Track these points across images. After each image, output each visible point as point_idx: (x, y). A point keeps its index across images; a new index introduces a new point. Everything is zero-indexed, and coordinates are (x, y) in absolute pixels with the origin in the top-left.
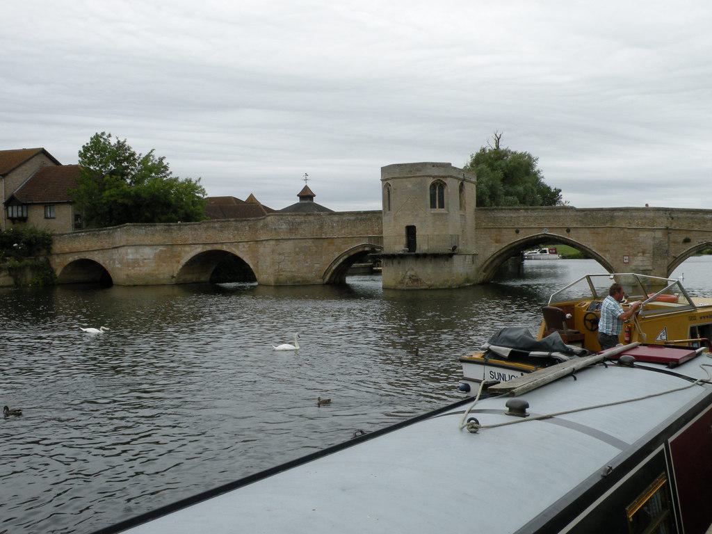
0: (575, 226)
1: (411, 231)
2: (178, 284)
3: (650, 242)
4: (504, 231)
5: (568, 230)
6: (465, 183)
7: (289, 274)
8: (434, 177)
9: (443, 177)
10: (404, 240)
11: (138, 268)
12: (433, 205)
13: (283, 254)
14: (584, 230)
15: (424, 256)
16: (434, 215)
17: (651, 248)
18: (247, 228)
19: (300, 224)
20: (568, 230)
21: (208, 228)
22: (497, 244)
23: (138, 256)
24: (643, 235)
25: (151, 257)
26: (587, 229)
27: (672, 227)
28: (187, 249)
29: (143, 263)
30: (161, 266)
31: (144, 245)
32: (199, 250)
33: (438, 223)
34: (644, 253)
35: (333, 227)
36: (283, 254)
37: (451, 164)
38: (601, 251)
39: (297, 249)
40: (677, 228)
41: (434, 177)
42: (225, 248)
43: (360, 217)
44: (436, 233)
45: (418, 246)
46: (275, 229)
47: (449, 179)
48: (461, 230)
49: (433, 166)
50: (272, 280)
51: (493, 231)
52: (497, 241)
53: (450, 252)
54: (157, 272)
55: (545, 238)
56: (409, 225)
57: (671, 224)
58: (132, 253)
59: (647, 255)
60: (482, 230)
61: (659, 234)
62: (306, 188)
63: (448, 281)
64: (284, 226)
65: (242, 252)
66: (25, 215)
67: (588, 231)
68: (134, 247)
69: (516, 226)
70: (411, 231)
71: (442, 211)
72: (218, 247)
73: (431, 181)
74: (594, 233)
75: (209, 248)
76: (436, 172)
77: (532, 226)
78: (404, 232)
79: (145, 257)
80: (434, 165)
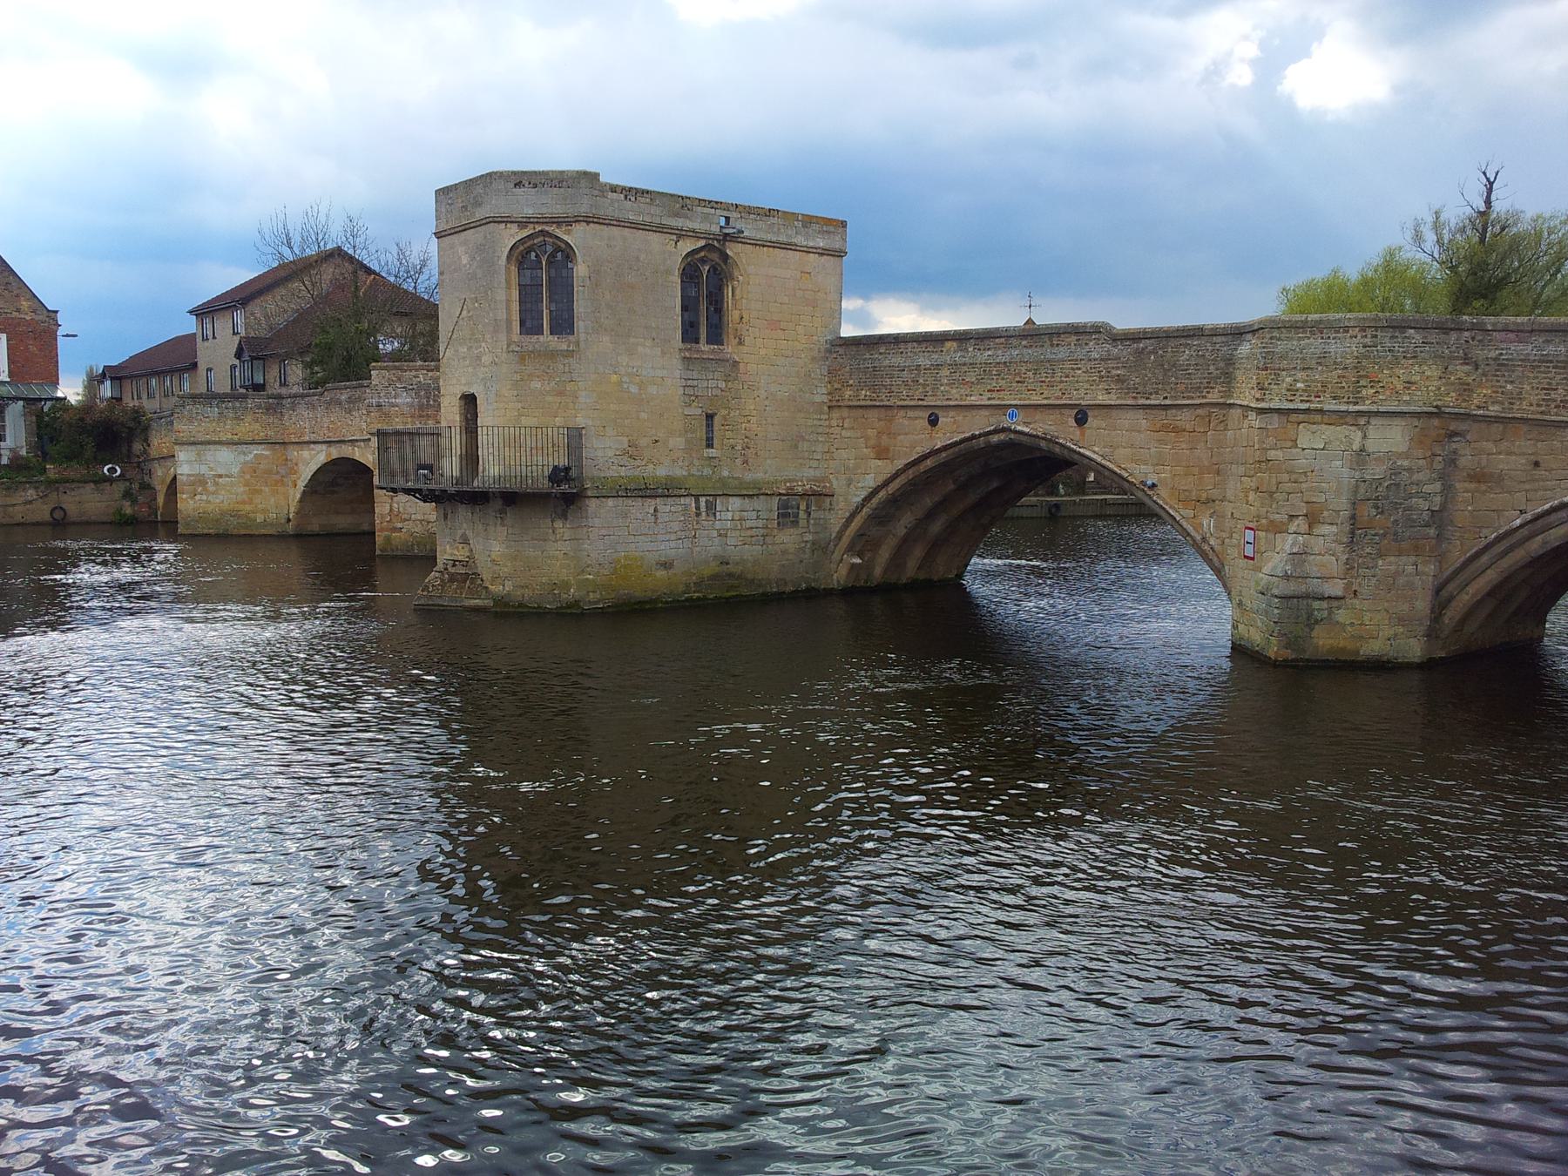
0: (1102, 398)
2: (300, 537)
3: (1340, 470)
4: (901, 419)
5: (1081, 420)
6: (732, 250)
7: (418, 529)
8: (522, 224)
11: (204, 497)
12: (530, 325)
14: (1131, 414)
17: (1342, 503)
20: (1081, 420)
22: (879, 463)
23: (204, 469)
24: (1311, 437)
25: (235, 470)
26: (1140, 413)
27: (1473, 405)
28: (306, 454)
29: (216, 484)
30: (259, 492)
31: (215, 443)
34: (1313, 519)
37: (597, 175)
40: (1494, 409)
44: (525, 421)
46: (379, 405)
47: (579, 229)
49: (518, 184)
51: (873, 415)
52: (882, 453)
54: (248, 508)
57: (1466, 389)
58: (189, 462)
59: (1326, 529)
60: (845, 412)
61: (1390, 439)
63: (566, 586)
64: (404, 399)
67: (1141, 420)
68: (193, 448)
69: (930, 401)
73: (510, 236)
74: (1165, 428)
75: (335, 452)
76: (528, 204)
77: (973, 400)
79: (220, 472)
80: (520, 180)
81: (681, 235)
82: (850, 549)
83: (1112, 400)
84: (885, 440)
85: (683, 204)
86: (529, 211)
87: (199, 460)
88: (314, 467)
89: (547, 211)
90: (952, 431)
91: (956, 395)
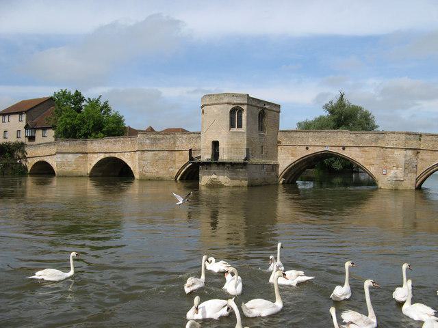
1: (216, 144)
5: (344, 149)
9: (241, 104)
10: (210, 151)
12: (232, 125)
15: (223, 164)
20: (344, 149)
24: (396, 152)
25: (73, 160)
28: (96, 156)
32: (102, 156)
35: (183, 143)
41: (234, 104)
42: (116, 156)
45: (220, 157)
48: (260, 146)
53: (242, 161)
55: (327, 154)
56: (215, 140)
64: (148, 141)
66: (33, 135)
70: (216, 144)
71: (240, 130)
72: (112, 155)
73: (231, 107)
75: (107, 155)
76: (235, 101)
77: (318, 144)
81: (259, 107)
82: (283, 177)
83: (351, 145)
85: (259, 101)
86: (235, 102)
88: (99, 159)
89: (239, 102)
90: (312, 151)
91: (313, 143)
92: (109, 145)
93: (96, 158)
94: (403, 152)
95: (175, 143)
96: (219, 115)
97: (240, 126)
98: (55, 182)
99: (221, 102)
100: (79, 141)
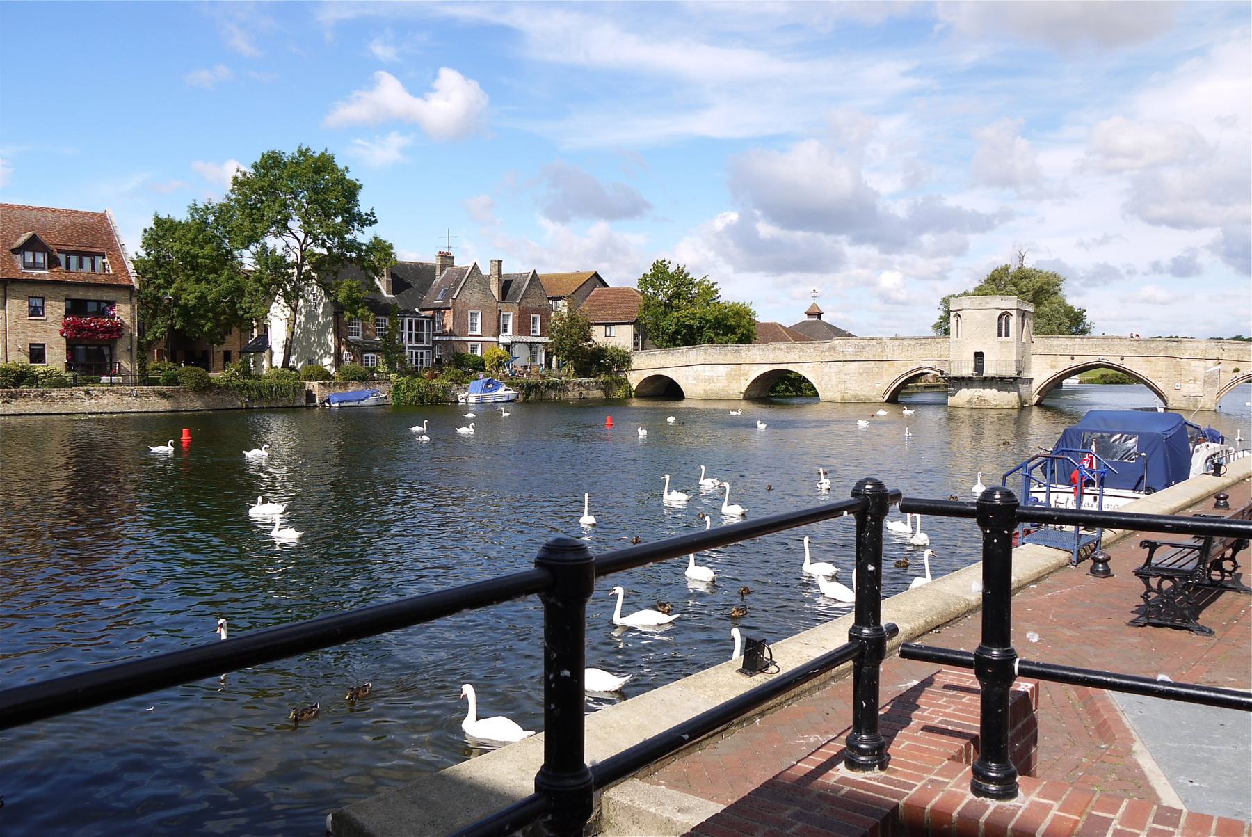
1: (979, 356)
3: (1201, 370)
5: (1122, 359)
7: (853, 393)
10: (972, 365)
12: (1000, 335)
13: (849, 374)
16: (1001, 342)
17: (1202, 377)
18: (812, 350)
19: (864, 347)
20: (1122, 359)
21: (775, 349)
23: (713, 374)
24: (1194, 363)
25: (724, 374)
28: (755, 367)
33: (1004, 350)
34: (1195, 381)
35: (894, 351)
36: (849, 374)
38: (1153, 378)
39: (861, 371)
42: (790, 368)
43: (920, 342)
45: (985, 371)
50: (838, 397)
52: (1052, 367)
57: (1222, 354)
62: (814, 306)
64: (851, 349)
65: (804, 371)
70: (979, 356)
73: (1000, 312)
78: (972, 358)
84: (1054, 363)
87: (712, 370)
92: (778, 353)
93: (756, 371)
94: (1203, 363)
95: (882, 351)
96: (984, 321)
97: (1007, 335)
98: (820, 403)
99: (988, 306)
100: (731, 347)
